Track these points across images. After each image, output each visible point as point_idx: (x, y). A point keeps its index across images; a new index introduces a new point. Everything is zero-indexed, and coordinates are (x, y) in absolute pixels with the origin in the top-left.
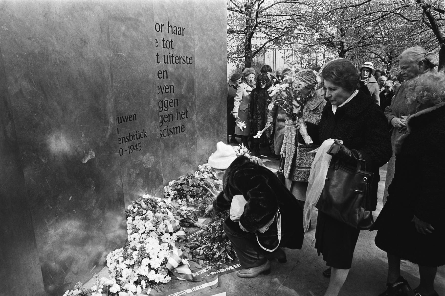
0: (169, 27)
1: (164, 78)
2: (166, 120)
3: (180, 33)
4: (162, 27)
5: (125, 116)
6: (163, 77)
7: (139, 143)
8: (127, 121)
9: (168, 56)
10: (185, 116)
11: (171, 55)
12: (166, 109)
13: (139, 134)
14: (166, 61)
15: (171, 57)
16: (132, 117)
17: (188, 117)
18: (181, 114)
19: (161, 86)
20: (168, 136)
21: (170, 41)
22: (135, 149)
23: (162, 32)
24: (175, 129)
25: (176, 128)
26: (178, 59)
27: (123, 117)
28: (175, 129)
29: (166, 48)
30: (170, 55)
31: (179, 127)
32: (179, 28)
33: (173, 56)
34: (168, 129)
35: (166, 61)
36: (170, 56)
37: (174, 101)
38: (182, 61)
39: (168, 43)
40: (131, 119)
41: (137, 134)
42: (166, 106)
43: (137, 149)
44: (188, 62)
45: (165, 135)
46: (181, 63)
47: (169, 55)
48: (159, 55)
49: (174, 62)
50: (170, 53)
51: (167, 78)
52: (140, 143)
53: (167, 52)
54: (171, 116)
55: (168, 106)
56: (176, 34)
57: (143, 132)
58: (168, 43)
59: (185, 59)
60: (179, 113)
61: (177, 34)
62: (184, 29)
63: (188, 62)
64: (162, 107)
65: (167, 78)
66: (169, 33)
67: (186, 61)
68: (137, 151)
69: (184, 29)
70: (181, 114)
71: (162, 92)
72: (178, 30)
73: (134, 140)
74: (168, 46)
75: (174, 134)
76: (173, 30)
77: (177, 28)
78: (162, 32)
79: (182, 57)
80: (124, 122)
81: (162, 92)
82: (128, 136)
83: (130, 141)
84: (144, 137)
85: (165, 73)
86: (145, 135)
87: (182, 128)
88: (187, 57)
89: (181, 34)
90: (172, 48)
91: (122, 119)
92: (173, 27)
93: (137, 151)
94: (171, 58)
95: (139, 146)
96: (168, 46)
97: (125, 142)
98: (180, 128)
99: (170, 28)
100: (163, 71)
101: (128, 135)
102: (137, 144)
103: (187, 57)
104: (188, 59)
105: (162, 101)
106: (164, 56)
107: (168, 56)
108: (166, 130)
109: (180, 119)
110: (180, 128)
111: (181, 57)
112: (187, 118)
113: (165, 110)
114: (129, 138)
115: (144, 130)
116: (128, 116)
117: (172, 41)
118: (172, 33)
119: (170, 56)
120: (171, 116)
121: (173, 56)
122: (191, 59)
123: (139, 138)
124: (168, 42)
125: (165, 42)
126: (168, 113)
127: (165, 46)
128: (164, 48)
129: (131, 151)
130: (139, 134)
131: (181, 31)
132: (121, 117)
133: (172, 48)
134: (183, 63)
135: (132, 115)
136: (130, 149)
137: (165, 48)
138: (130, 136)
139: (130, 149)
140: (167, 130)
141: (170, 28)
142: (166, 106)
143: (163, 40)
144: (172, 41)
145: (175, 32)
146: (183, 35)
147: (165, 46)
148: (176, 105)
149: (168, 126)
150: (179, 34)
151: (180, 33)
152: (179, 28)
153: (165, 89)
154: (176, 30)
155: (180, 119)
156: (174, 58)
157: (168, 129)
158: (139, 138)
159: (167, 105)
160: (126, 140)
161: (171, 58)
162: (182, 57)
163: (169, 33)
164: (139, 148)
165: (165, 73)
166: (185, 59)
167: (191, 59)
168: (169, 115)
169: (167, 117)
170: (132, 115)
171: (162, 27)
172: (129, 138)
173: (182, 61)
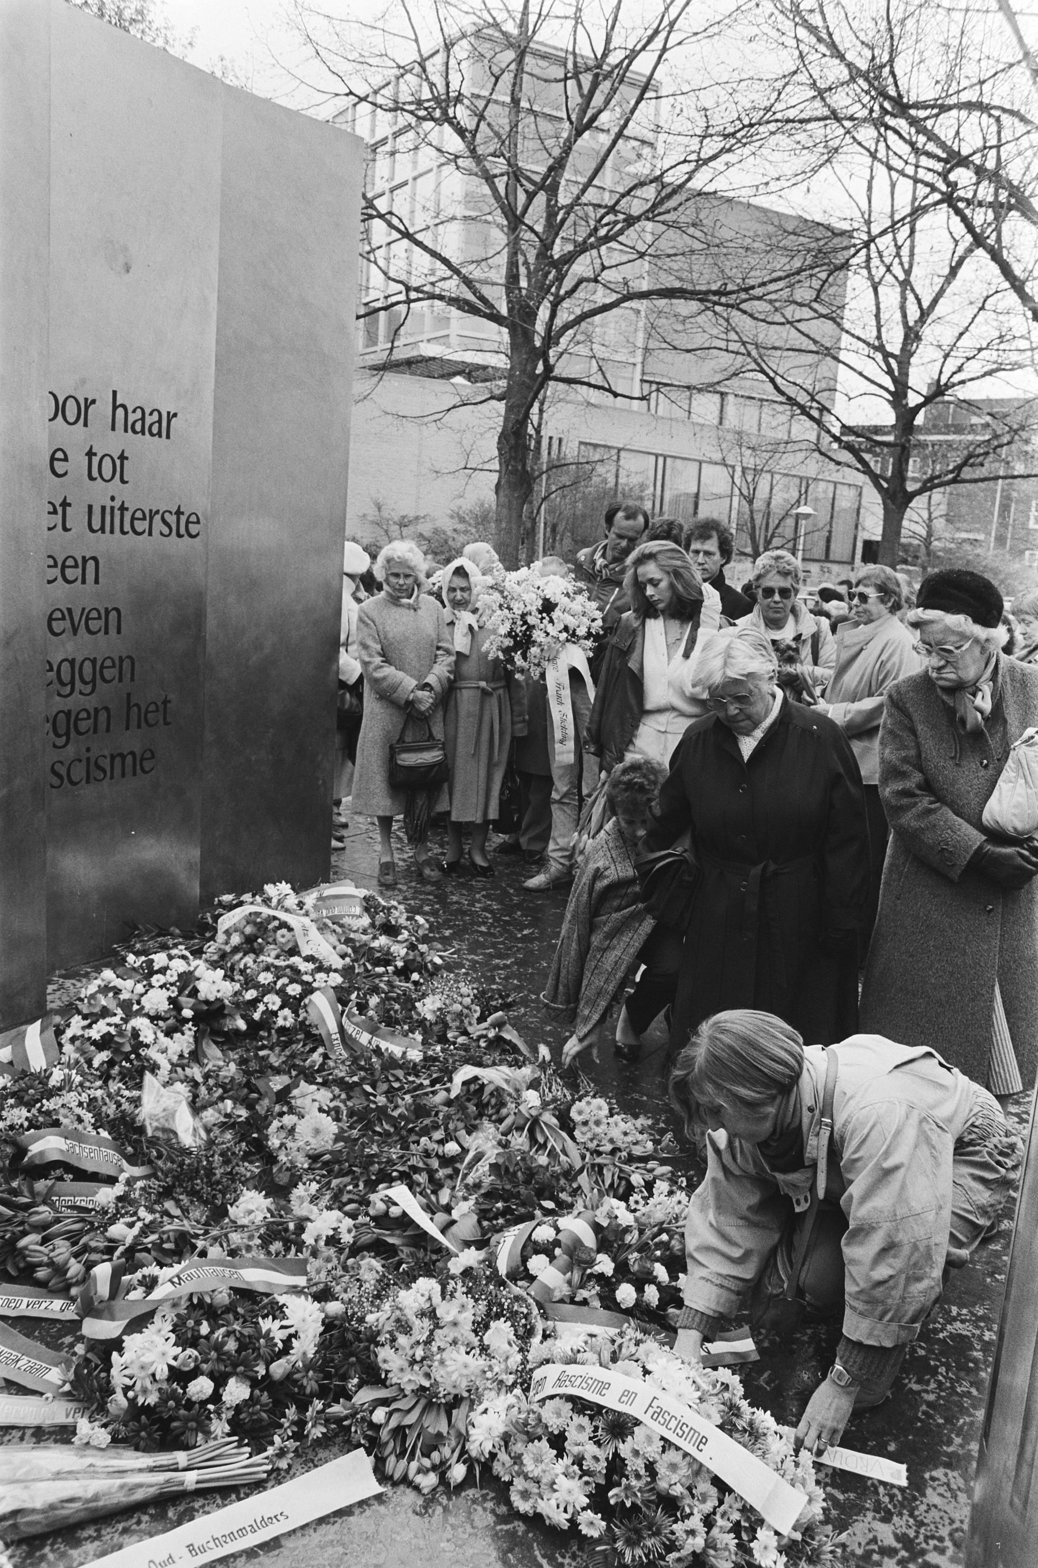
0: (115, 408)
1: (84, 582)
2: (83, 726)
3: (155, 430)
4: (87, 408)
6: (80, 580)
9: (103, 508)
11: (117, 504)
12: (88, 689)
14: (96, 526)
17: (169, 720)
18: (143, 711)
19: (69, 610)
20: (88, 782)
23: (86, 425)
24: (118, 760)
25: (123, 757)
26: (144, 518)
28: (118, 760)
31: (132, 753)
32: (156, 414)
34: (88, 759)
35: (96, 526)
36: (112, 508)
38: (158, 525)
39: (107, 463)
42: (88, 677)
44: (182, 531)
45: (75, 779)
47: (109, 504)
48: (69, 505)
49: (127, 527)
50: (113, 499)
53: (100, 493)
54: (103, 716)
55: (94, 680)
56: (143, 432)
58: (107, 463)
59: (172, 519)
60: (137, 705)
61: (143, 434)
62: (175, 415)
63: (182, 531)
64: (72, 682)
65: (97, 582)
66: (113, 429)
71: (75, 631)
72: (149, 420)
74: (107, 473)
75: (112, 777)
76: (132, 418)
77: (147, 412)
78: (86, 425)
81: (75, 631)
85: (91, 564)
87: (142, 759)
89: (159, 434)
90: (123, 481)
92: (130, 410)
94: (117, 513)
96: (107, 473)
99: (120, 412)
100: (84, 558)
103: (179, 513)
105: (74, 660)
106: (90, 507)
108: (80, 761)
109: (139, 727)
111: (157, 512)
112: (166, 723)
113: (81, 693)
117: (123, 457)
118: (126, 431)
119: (112, 508)
120: (103, 716)
122: (193, 518)
124: (107, 459)
125: (95, 461)
126: (92, 702)
127: (95, 473)
128: (91, 478)
131: (160, 421)
133: (123, 481)
140: (84, 762)
141: (120, 412)
142: (88, 677)
143: (90, 454)
144: (123, 457)
146: (168, 437)
147: (95, 473)
149: (88, 750)
150: (152, 435)
151: (155, 430)
152: (156, 414)
153: (88, 619)
154: (143, 419)
155: (139, 727)
157: (88, 759)
161: (117, 513)
163: (113, 429)
165: (91, 564)
166: (172, 519)
167: (193, 518)
168: (96, 710)
169: (89, 718)
171: (87, 408)
173: (158, 525)
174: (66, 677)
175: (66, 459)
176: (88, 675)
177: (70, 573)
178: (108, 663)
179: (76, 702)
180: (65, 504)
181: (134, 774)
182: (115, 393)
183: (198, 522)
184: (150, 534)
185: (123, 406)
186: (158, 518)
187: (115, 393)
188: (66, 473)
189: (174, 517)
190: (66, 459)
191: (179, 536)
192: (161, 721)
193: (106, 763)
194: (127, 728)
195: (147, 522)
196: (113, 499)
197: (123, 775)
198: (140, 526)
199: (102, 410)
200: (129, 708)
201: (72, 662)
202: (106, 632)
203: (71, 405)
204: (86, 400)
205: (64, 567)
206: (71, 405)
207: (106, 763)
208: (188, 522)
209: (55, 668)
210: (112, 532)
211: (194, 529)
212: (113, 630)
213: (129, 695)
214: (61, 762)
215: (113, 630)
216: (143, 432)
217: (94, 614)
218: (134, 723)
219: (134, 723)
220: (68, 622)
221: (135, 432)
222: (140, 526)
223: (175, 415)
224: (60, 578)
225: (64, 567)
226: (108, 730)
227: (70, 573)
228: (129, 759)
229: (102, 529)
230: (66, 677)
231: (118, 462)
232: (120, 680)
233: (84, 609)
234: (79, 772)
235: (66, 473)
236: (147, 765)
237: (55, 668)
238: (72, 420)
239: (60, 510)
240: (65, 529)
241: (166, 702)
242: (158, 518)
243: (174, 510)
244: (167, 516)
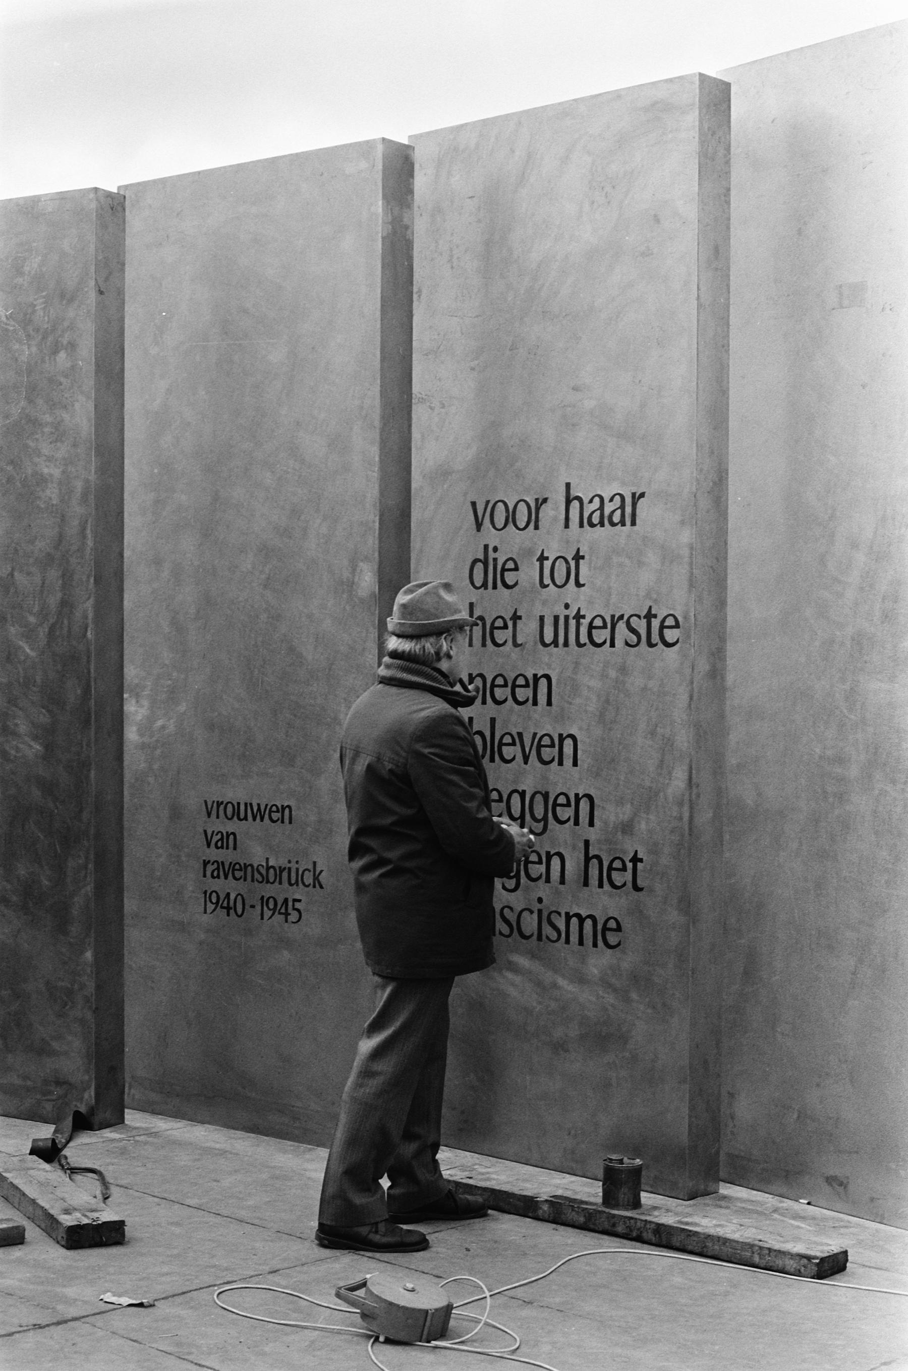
0: (568, 502)
1: (535, 703)
3: (617, 518)
5: (259, 805)
6: (531, 701)
7: (295, 900)
8: (262, 819)
9: (556, 618)
10: (629, 875)
11: (572, 612)
12: (539, 827)
13: (297, 870)
14: (549, 637)
15: (571, 617)
16: (278, 811)
18: (606, 865)
19: (520, 735)
22: (280, 913)
23: (536, 527)
26: (605, 627)
27: (251, 804)
29: (552, 585)
30: (567, 612)
33: (579, 617)
35: (549, 637)
36: (567, 618)
37: (573, 803)
39: (561, 567)
40: (275, 816)
41: (290, 869)
42: (539, 812)
43: (287, 914)
44: (655, 638)
46: (619, 642)
47: (562, 612)
49: (584, 639)
50: (567, 606)
51: (549, 703)
52: (300, 901)
55: (545, 819)
56: (602, 524)
57: (311, 867)
58: (561, 567)
63: (655, 638)
65: (549, 703)
66: (567, 526)
67: (643, 632)
68: (286, 921)
69: (636, 498)
70: (606, 865)
71: (526, 759)
72: (607, 510)
73: (280, 883)
74: (560, 578)
78: (536, 527)
79: (626, 618)
80: (254, 819)
81: (526, 759)
82: (263, 866)
83: (268, 882)
84: (314, 886)
85: (543, 683)
86: (316, 878)
88: (650, 616)
90: (578, 584)
91: (249, 808)
92: (586, 501)
93: (286, 921)
94: (573, 623)
95: (294, 909)
97: (253, 880)
98: (600, 927)
100: (535, 675)
101: (264, 864)
102: (286, 901)
103: (650, 616)
104: (656, 623)
105: (524, 792)
107: (556, 618)
110: (600, 927)
111: (621, 617)
112: (636, 888)
114: (264, 872)
115: (315, 863)
116: (267, 805)
117: (578, 557)
118: (581, 525)
119: (567, 618)
121: (579, 617)
122: (670, 622)
123: (297, 883)
125: (547, 564)
127: (547, 581)
129: (268, 913)
130: (297, 870)
131: (622, 507)
132: (246, 804)
133: (578, 584)
134: (627, 644)
135: (280, 807)
136: (265, 908)
137: (548, 586)
138: (268, 868)
139: (265, 908)
143: (542, 559)
145: (596, 519)
146: (633, 523)
147: (547, 581)
150: (613, 524)
151: (617, 518)
152: (618, 498)
153: (539, 746)
154: (601, 508)
155: (601, 885)
158: (297, 883)
159: (519, 809)
160: (257, 876)
161: (573, 623)
162: (626, 618)
163: (567, 526)
164: (294, 916)
167: (670, 622)
170: (280, 807)
171: (538, 509)
172: (264, 872)
175: (516, 569)
176: (539, 812)
177: (521, 694)
178: (562, 800)
180: (516, 618)
181: (595, 945)
182: (568, 485)
183: (677, 626)
184: (612, 645)
185: (579, 499)
186: (622, 626)
187: (568, 485)
188: (516, 584)
189: (644, 622)
190: (516, 569)
191: (651, 645)
192: (629, 885)
194: (586, 884)
195: (608, 631)
196: (567, 606)
197: (581, 943)
198: (601, 636)
200: (587, 859)
201: (523, 794)
202: (561, 763)
203: (522, 509)
204: (537, 500)
205: (514, 686)
206: (522, 509)
208: (662, 627)
209: (505, 797)
210: (566, 644)
211: (670, 636)
212: (568, 762)
213: (587, 843)
214: (511, 909)
215: (568, 762)
216: (602, 524)
217: (546, 741)
220: (518, 747)
221: (592, 525)
223: (642, 495)
224: (510, 698)
225: (514, 686)
226: (562, 881)
227: (521, 694)
229: (555, 643)
231: (573, 564)
232: (577, 823)
233: (535, 734)
235: (516, 584)
236: (612, 939)
237: (505, 797)
238: (522, 525)
239: (510, 624)
240: (516, 645)
242: (621, 626)
243: (643, 614)
244: (634, 620)
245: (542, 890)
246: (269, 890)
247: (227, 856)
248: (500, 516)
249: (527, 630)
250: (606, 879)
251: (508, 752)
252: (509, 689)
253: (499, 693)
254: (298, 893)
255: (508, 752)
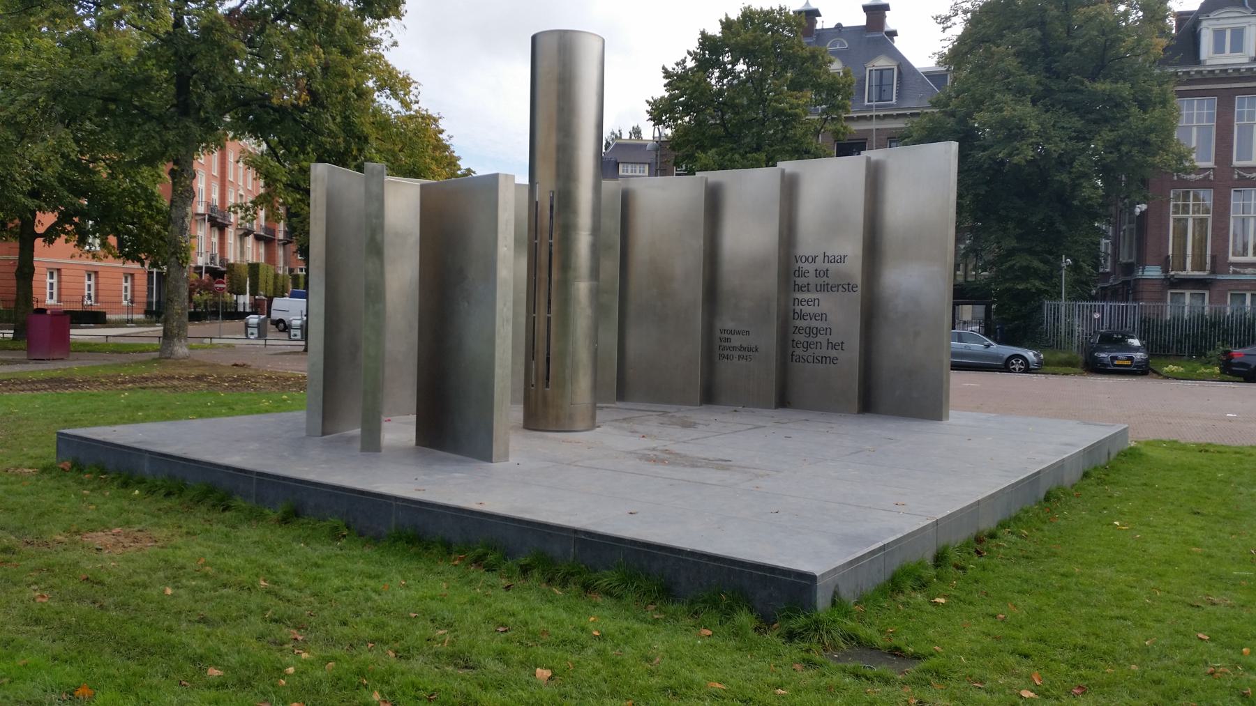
14: (819, 289)
21: (825, 270)
24: (824, 359)
28: (824, 359)
33: (828, 284)
35: (819, 289)
42: (815, 332)
53: (820, 281)
88: (849, 284)
103: (849, 284)
104: (851, 286)
121: (828, 284)
126: (816, 340)
143: (816, 270)
148: (828, 333)
156: (829, 287)
164: (749, 360)
165: (817, 301)
166: (847, 287)
174: (808, 332)
176: (815, 332)
177: (810, 303)
179: (810, 340)
193: (820, 359)
198: (834, 289)
199: (821, 257)
203: (810, 258)
206: (810, 258)
207: (820, 359)
218: (830, 348)
219: (830, 348)
222: (834, 289)
228: (828, 359)
230: (808, 332)
234: (810, 359)
236: (835, 362)
241: (842, 343)
245: (814, 350)
246: (740, 353)
247: (727, 344)
248: (804, 259)
249: (812, 287)
250: (834, 347)
251: (805, 318)
252: (805, 303)
253: (803, 303)
254: (751, 353)
255: (805, 318)
